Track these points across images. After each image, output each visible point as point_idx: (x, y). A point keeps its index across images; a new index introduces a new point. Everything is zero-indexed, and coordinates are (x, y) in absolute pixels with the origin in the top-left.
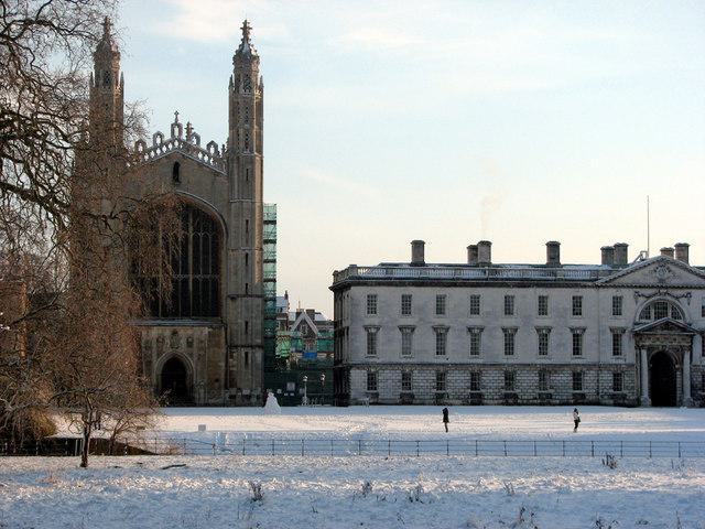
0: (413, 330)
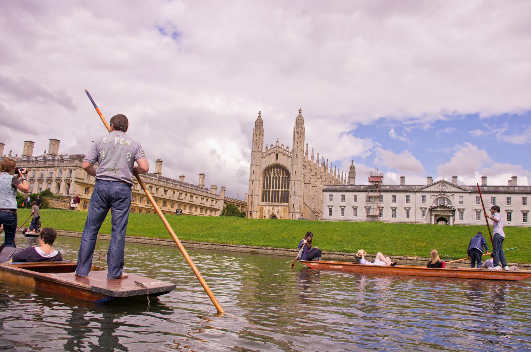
0: (345, 207)
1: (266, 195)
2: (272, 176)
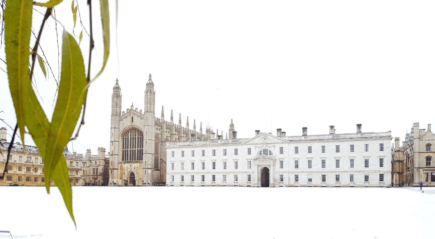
1: (125, 155)
2: (129, 137)
